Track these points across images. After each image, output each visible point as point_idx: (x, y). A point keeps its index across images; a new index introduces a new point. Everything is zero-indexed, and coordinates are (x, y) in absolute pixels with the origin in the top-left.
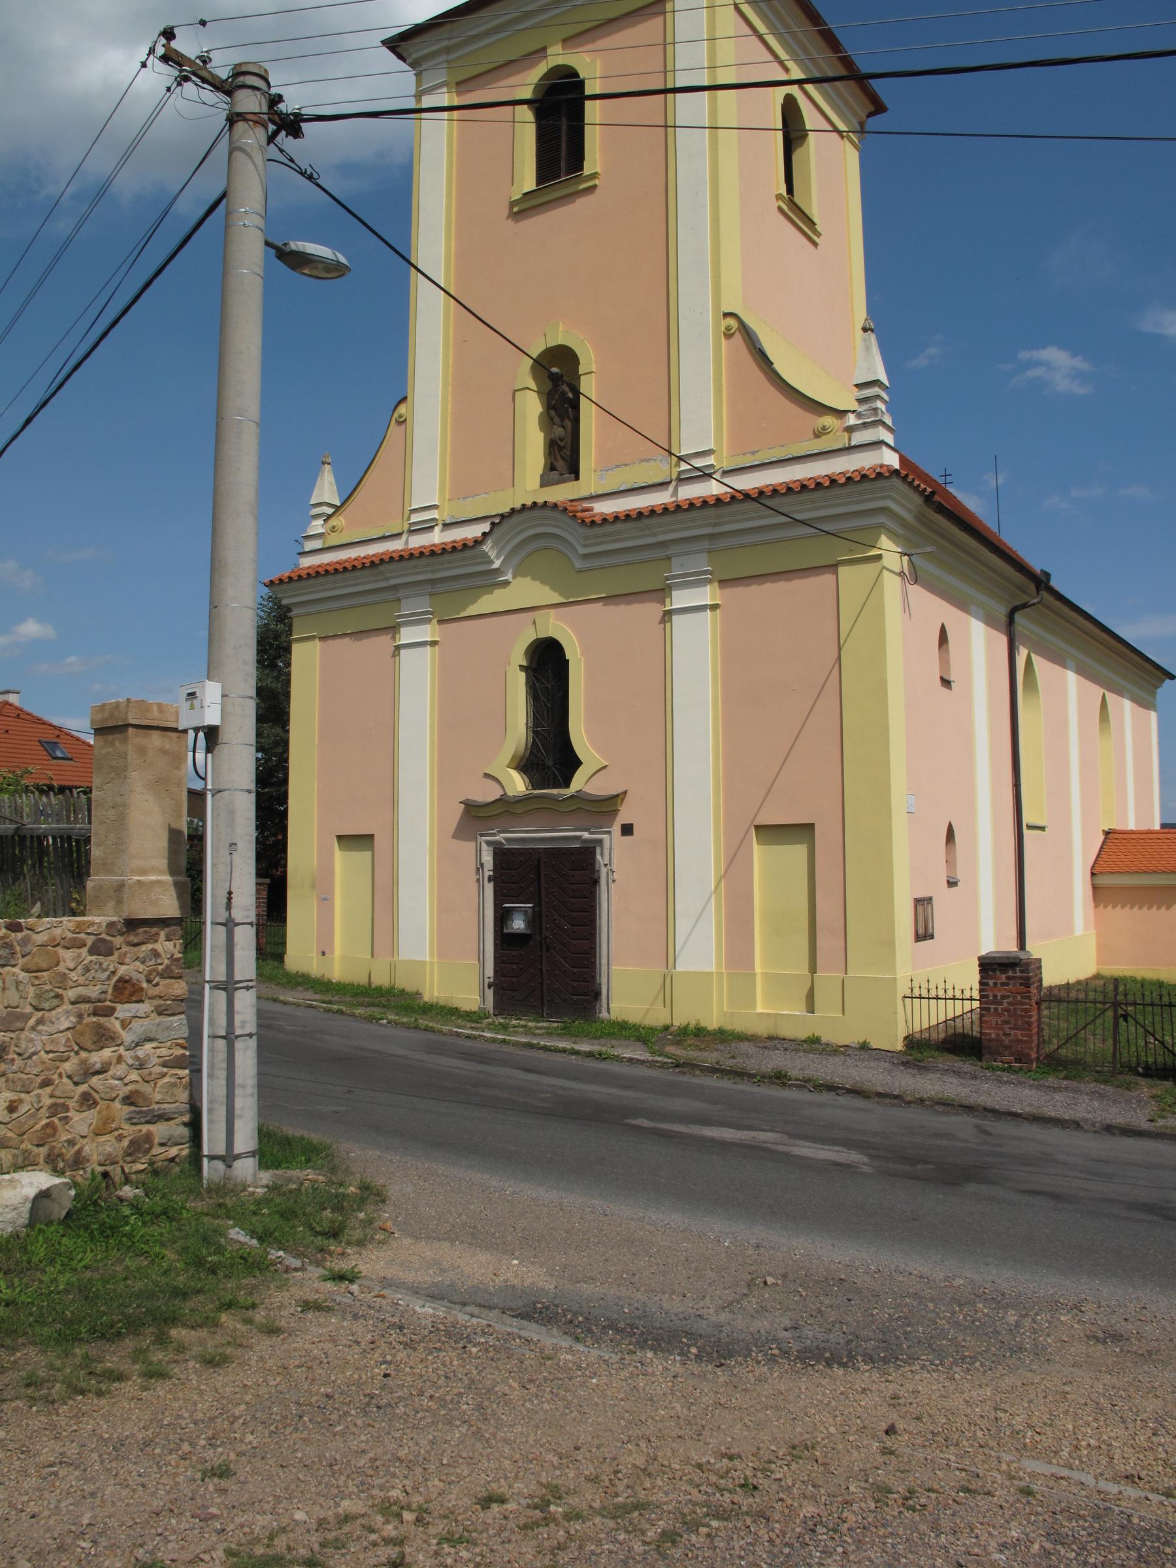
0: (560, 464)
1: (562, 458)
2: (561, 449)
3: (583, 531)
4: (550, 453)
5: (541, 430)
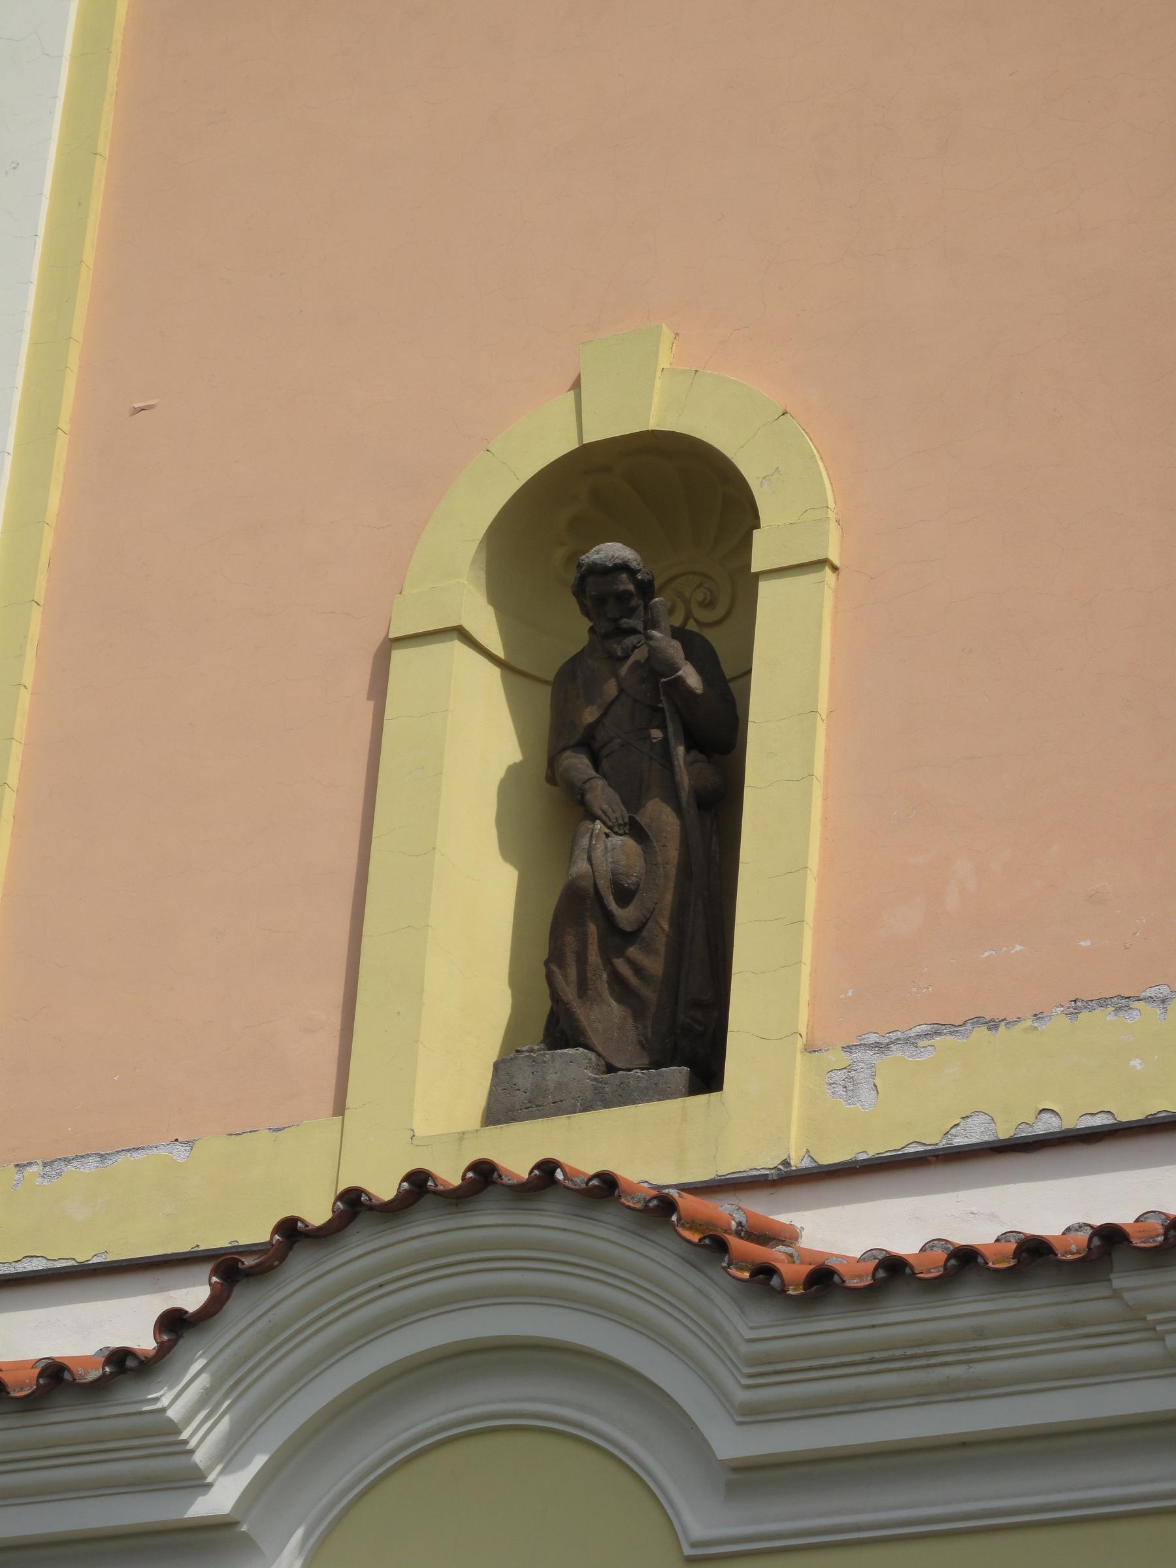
0: (605, 1016)
1: (621, 989)
2: (618, 938)
3: (755, 1328)
4: (555, 957)
5: (508, 851)
